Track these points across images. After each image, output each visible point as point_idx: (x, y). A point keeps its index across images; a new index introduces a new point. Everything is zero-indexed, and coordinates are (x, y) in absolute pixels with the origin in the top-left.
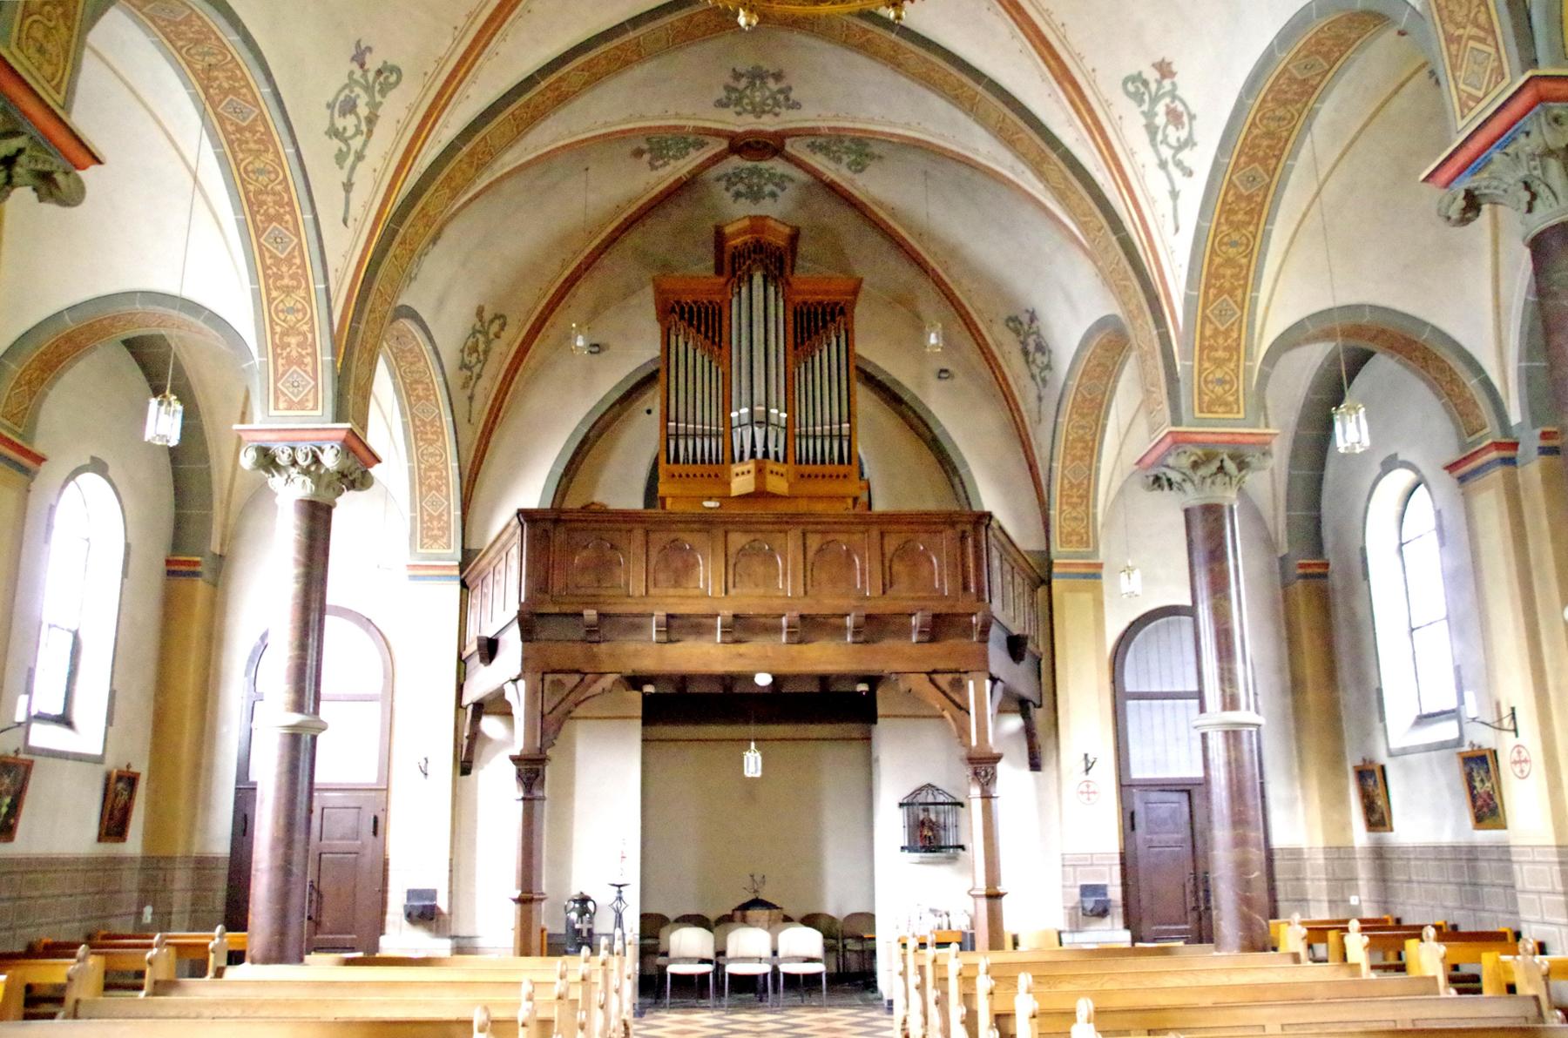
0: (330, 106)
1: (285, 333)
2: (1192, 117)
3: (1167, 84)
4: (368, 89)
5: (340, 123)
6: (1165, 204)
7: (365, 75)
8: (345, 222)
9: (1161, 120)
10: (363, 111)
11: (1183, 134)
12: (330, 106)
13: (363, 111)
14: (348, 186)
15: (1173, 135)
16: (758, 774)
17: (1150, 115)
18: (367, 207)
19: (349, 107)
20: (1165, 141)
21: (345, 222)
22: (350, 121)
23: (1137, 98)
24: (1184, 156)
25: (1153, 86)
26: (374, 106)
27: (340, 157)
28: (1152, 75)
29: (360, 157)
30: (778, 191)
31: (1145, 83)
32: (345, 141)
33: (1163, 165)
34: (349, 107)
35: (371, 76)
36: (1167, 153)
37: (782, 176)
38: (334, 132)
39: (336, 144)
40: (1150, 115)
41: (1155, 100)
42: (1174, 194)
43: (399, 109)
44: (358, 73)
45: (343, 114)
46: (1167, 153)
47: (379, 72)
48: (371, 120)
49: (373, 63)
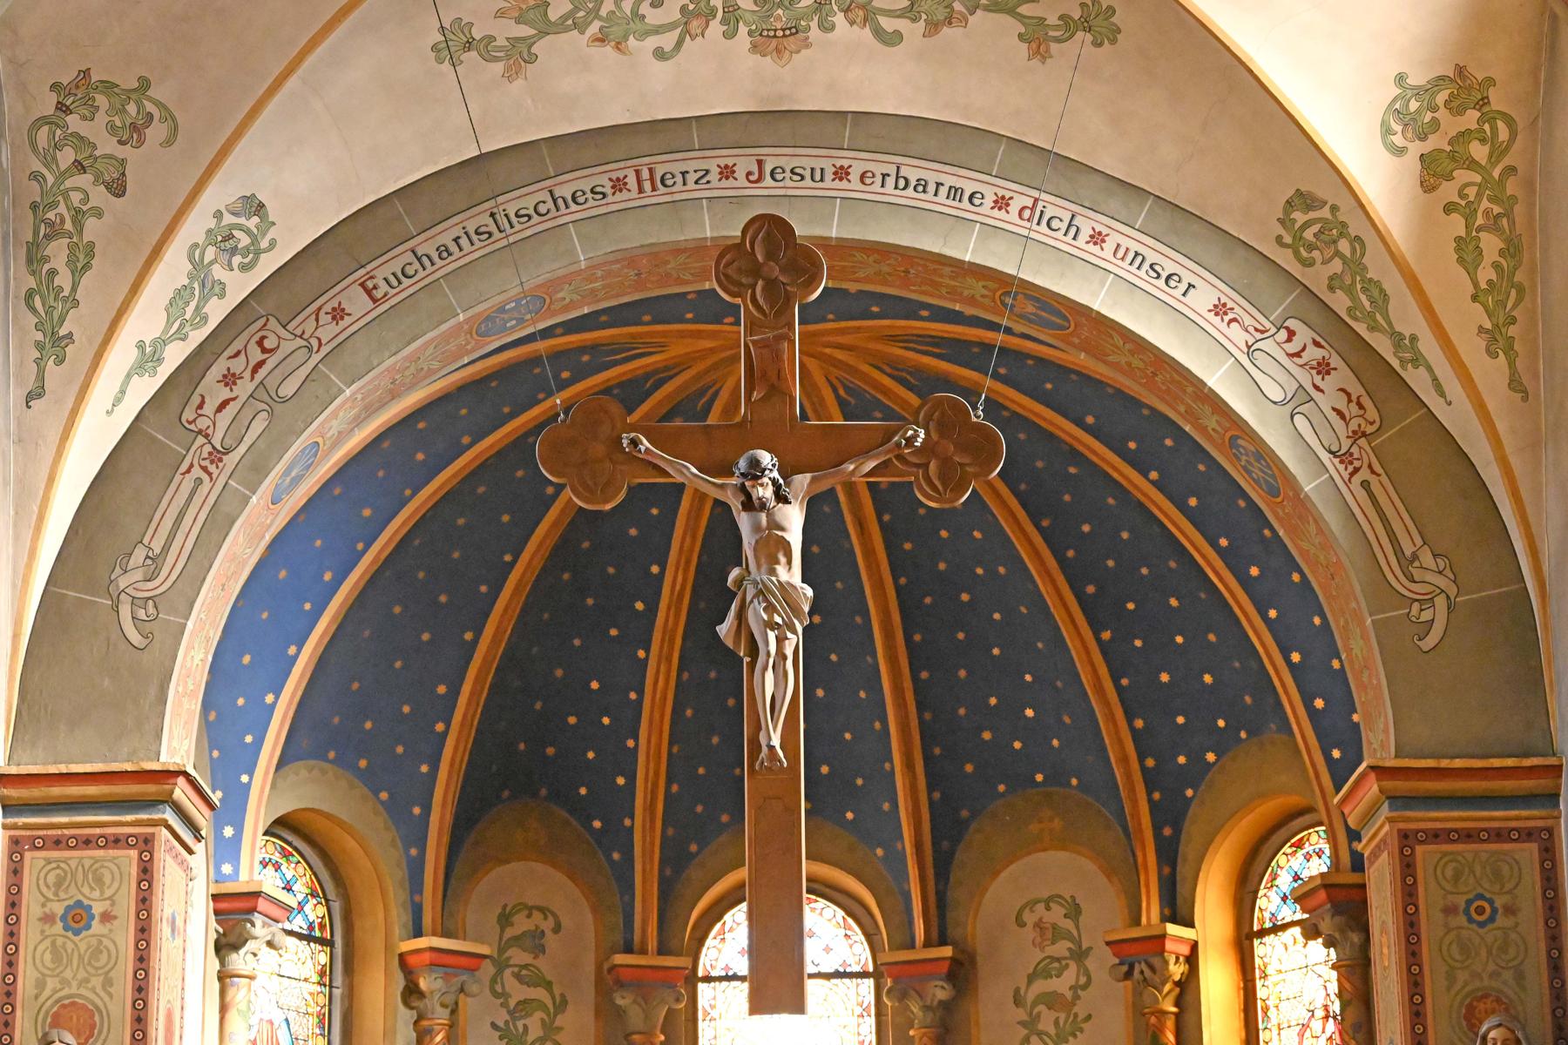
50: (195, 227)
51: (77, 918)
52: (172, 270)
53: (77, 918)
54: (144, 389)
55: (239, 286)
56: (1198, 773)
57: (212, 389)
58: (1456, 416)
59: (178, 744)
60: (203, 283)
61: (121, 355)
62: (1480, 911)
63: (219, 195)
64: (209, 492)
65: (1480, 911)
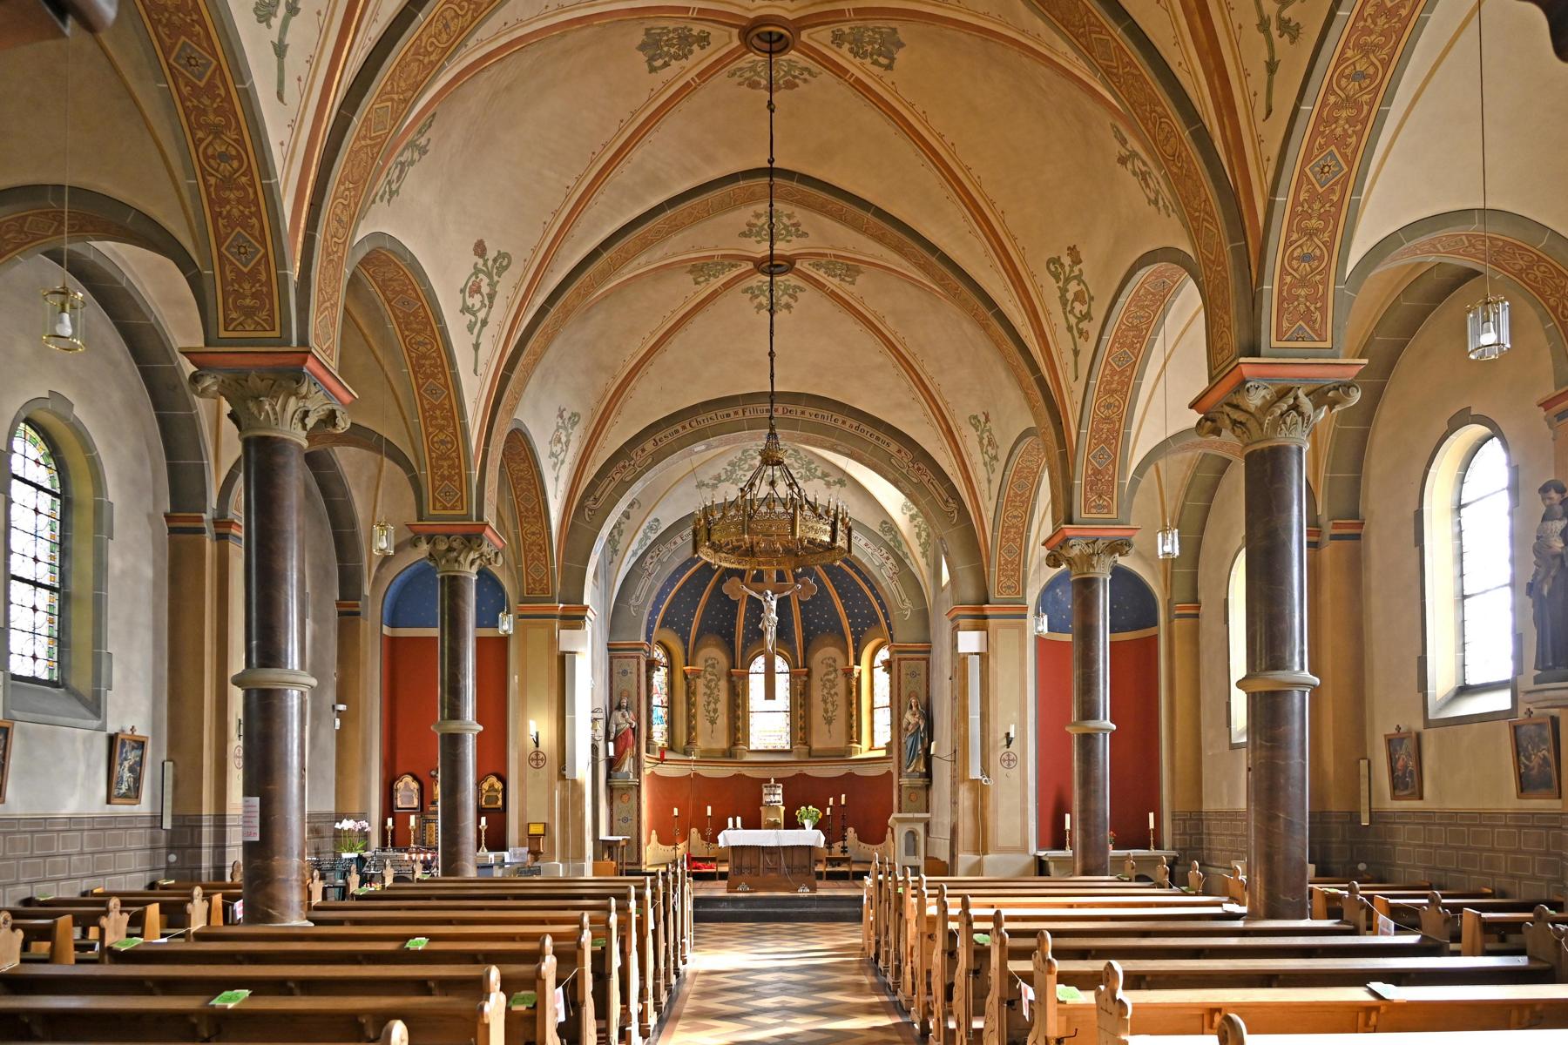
0: (462, 291)
1: (440, 458)
2: (1092, 298)
3: (1076, 269)
4: (489, 275)
5: (470, 302)
6: (1069, 356)
7: (485, 264)
8: (475, 372)
9: (1070, 296)
10: (485, 289)
11: (1085, 309)
12: (462, 291)
13: (485, 289)
14: (476, 347)
15: (1078, 307)
16: (783, 742)
17: (1063, 291)
18: (488, 364)
19: (476, 290)
20: (1072, 311)
21: (475, 372)
22: (478, 297)
23: (1057, 277)
24: (1084, 325)
25: (1067, 269)
26: (492, 285)
27: (470, 328)
28: (1066, 261)
29: (484, 323)
30: (791, 301)
31: (1062, 265)
32: (474, 314)
33: (1070, 329)
34: (476, 290)
35: (490, 263)
36: (1073, 320)
37: (796, 287)
38: (466, 309)
39: (469, 317)
40: (1063, 291)
41: (1067, 280)
42: (1076, 353)
43: (508, 287)
44: (481, 262)
45: (471, 296)
46: (1073, 320)
47: (495, 260)
48: (491, 297)
49: (491, 254)
50: (644, 526)
51: (625, 673)
52: (640, 535)
53: (625, 673)
54: (634, 560)
55: (653, 536)
56: (863, 632)
57: (648, 560)
58: (914, 569)
59: (643, 639)
60: (646, 537)
61: (629, 553)
62: (914, 675)
63: (650, 519)
64: (649, 583)
65: (914, 675)
